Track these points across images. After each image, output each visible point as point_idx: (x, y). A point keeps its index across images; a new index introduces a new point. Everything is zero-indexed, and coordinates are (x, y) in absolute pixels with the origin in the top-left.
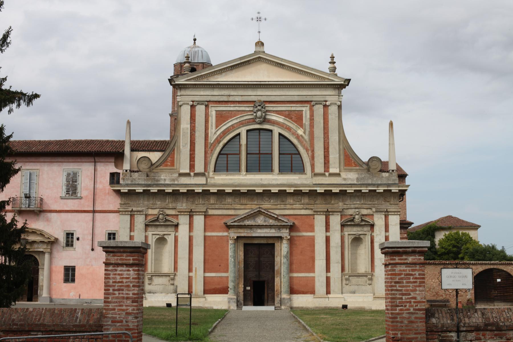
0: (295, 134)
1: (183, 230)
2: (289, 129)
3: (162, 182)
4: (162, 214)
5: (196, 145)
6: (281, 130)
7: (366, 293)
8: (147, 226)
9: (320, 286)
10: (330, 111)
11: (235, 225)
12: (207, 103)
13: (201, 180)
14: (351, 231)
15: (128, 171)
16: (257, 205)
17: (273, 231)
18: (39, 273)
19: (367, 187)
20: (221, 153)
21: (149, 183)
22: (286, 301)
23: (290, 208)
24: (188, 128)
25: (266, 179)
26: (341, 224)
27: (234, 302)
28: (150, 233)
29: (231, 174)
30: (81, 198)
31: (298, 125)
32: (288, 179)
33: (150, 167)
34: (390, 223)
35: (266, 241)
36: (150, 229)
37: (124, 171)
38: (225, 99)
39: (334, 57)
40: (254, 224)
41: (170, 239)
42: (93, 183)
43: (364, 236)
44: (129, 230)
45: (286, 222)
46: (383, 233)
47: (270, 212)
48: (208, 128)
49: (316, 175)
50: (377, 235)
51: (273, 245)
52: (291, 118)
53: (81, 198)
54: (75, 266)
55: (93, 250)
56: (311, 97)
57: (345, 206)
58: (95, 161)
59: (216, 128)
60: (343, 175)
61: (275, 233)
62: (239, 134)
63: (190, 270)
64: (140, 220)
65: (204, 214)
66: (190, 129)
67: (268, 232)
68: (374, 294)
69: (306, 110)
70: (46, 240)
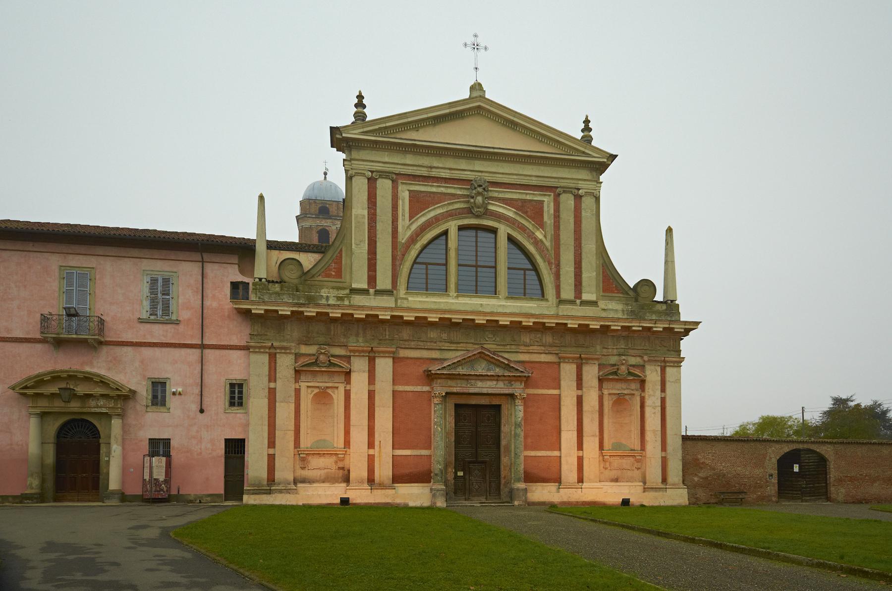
0: (531, 236)
1: (359, 382)
2: (522, 229)
3: (324, 302)
4: (324, 353)
5: (378, 244)
6: (510, 229)
7: (633, 482)
8: (297, 372)
9: (569, 471)
10: (583, 206)
11: (443, 374)
12: (395, 177)
13: (387, 302)
14: (612, 389)
15: (263, 280)
16: (475, 344)
17: (501, 384)
18: (101, 452)
19: (640, 323)
20: (417, 261)
21: (301, 302)
23: (526, 351)
24: (364, 216)
25: (488, 305)
26: (599, 378)
27: (443, 495)
28: (303, 385)
29: (434, 295)
30: (177, 323)
31: (537, 224)
32: (521, 306)
33: (301, 277)
34: (667, 379)
36: (303, 378)
37: (257, 280)
38: (424, 172)
39: (589, 121)
40: (473, 373)
41: (338, 397)
42: (200, 297)
43: (630, 396)
44: (267, 378)
45: (522, 372)
46: (658, 393)
47: (498, 356)
48: (397, 219)
49: (561, 302)
50: (650, 396)
51: (498, 408)
52: (526, 213)
53: (177, 323)
54: (170, 439)
55: (202, 411)
56: (556, 180)
57: (605, 350)
58: (203, 259)
59: (410, 221)
60: (602, 304)
62: (445, 233)
63: (371, 445)
64: (285, 363)
65: (392, 355)
66: (368, 217)
67: (494, 386)
68: (645, 483)
69: (548, 201)
70: (113, 393)
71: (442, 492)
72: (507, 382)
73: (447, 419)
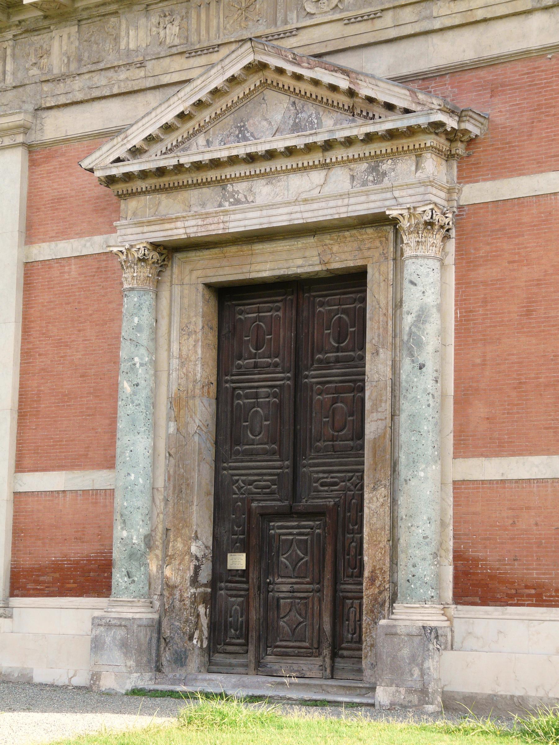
22: (405, 652)
23: (457, 22)
27: (124, 645)
35: (316, 260)
45: (407, 111)
61: (348, 195)
67: (315, 193)
71: (121, 633)
72: (364, 166)
73: (175, 347)
